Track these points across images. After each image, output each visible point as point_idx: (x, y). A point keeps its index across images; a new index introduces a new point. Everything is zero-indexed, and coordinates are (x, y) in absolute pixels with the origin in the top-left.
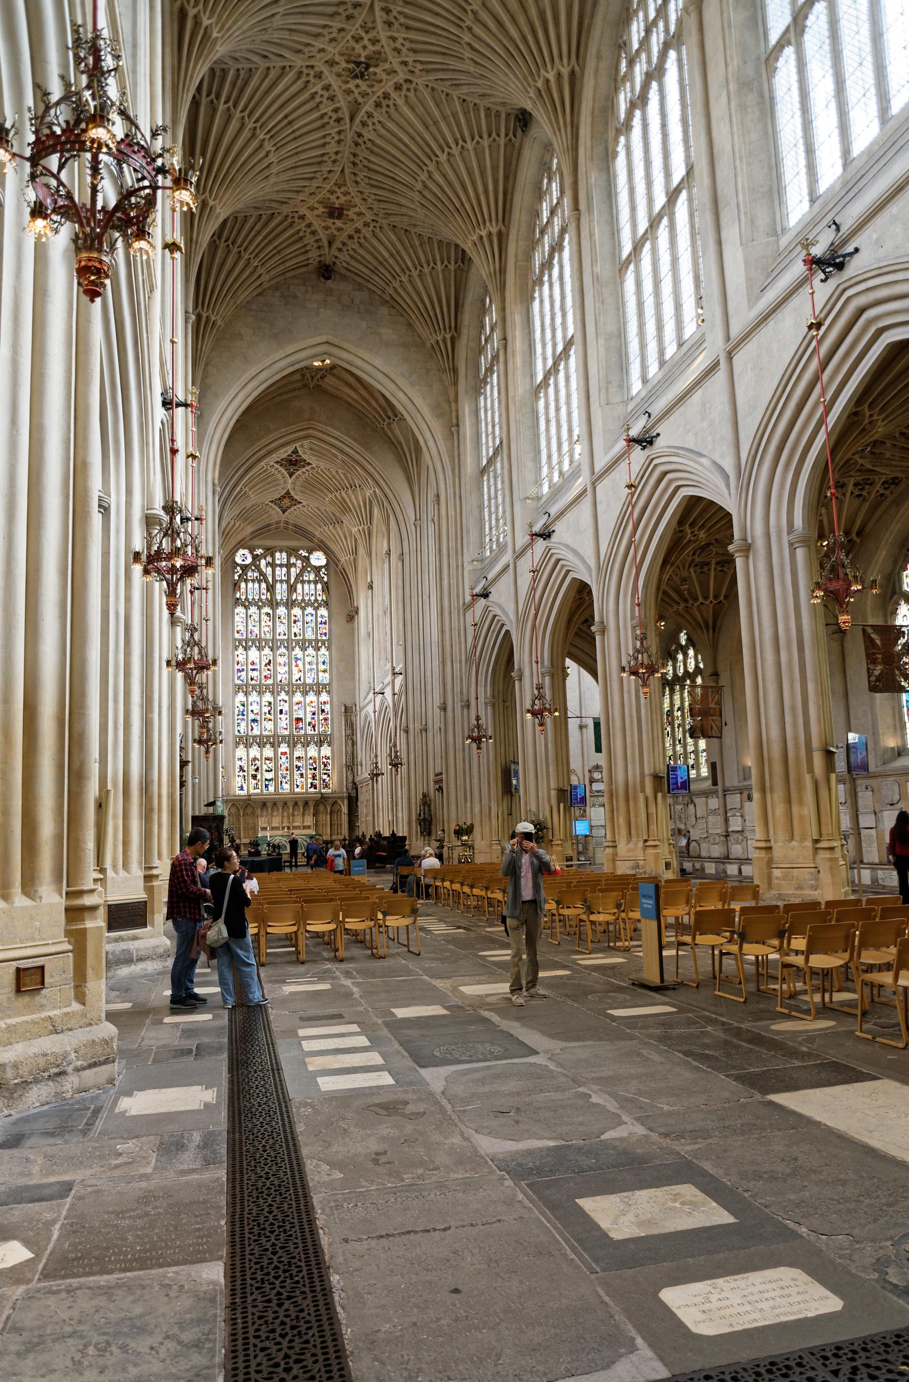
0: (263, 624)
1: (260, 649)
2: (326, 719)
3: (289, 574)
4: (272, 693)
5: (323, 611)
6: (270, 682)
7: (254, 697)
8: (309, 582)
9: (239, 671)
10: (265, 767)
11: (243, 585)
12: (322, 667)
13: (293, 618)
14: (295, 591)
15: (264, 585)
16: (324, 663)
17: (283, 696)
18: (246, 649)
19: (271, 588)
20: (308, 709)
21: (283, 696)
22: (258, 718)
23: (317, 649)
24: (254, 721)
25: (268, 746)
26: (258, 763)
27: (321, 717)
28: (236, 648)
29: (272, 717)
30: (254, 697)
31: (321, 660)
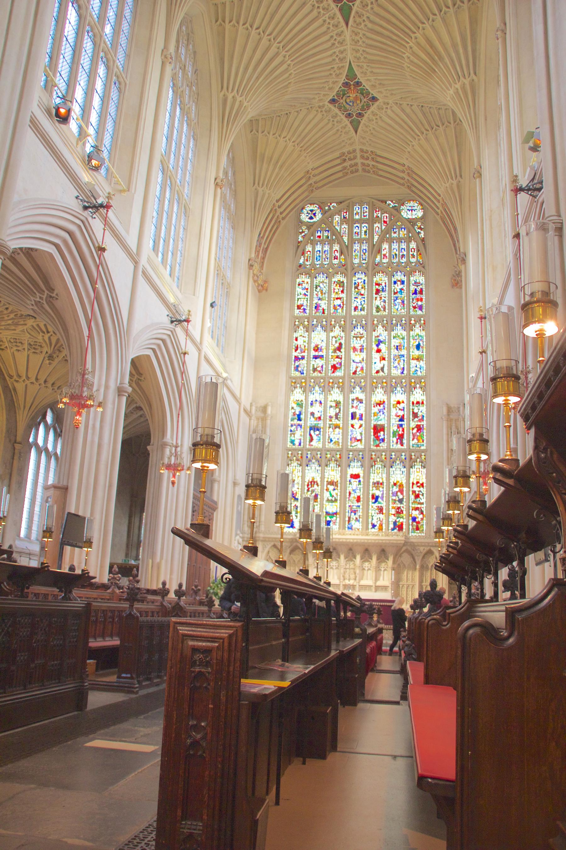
0: (333, 295)
1: (328, 328)
2: (419, 428)
3: (371, 231)
4: (342, 388)
5: (419, 278)
6: (338, 373)
7: (317, 395)
8: (399, 240)
9: (297, 358)
10: (327, 495)
11: (309, 248)
12: (417, 353)
13: (375, 287)
14: (379, 251)
15: (336, 247)
16: (418, 347)
17: (358, 393)
18: (309, 329)
19: (346, 250)
20: (394, 411)
21: (358, 393)
22: (321, 424)
23: (409, 327)
24: (315, 428)
25: (333, 464)
26: (317, 489)
27: (413, 425)
28: (295, 328)
29: (340, 423)
30: (317, 395)
31: (414, 343)
